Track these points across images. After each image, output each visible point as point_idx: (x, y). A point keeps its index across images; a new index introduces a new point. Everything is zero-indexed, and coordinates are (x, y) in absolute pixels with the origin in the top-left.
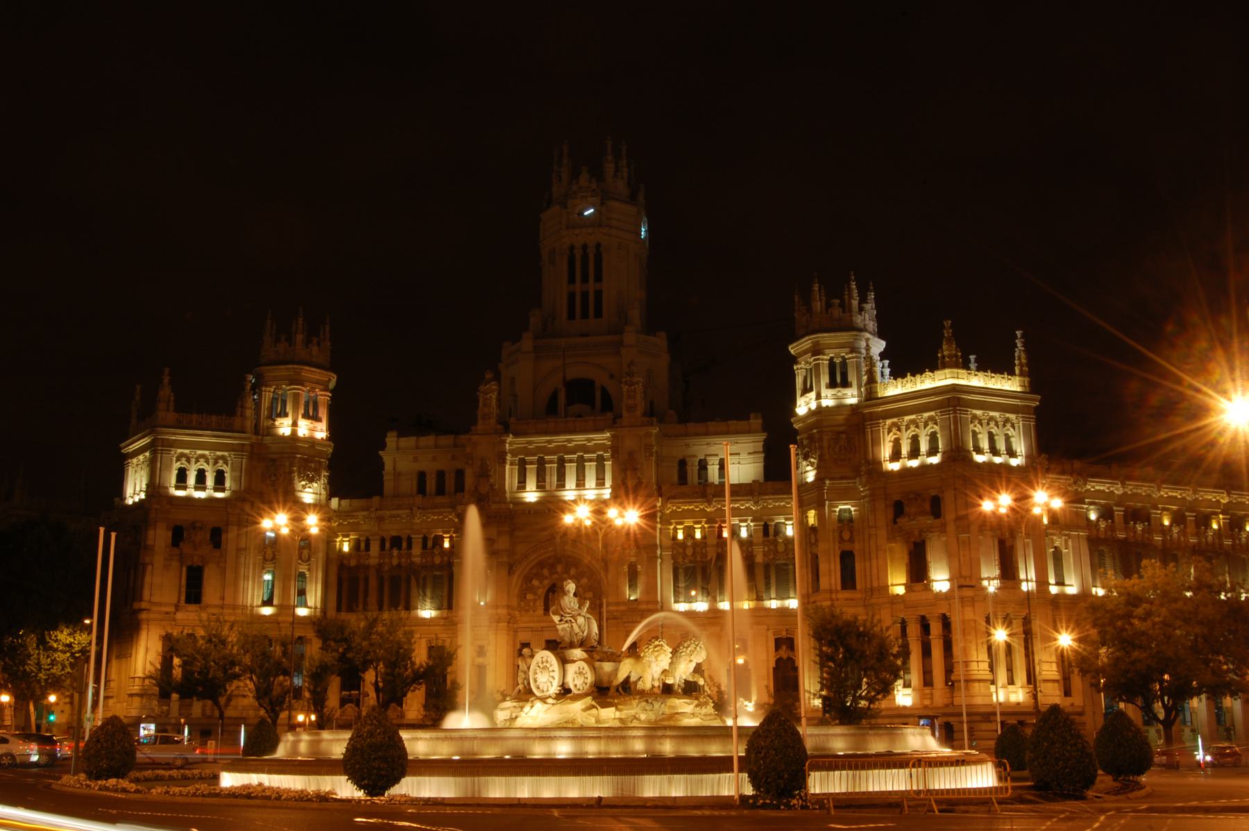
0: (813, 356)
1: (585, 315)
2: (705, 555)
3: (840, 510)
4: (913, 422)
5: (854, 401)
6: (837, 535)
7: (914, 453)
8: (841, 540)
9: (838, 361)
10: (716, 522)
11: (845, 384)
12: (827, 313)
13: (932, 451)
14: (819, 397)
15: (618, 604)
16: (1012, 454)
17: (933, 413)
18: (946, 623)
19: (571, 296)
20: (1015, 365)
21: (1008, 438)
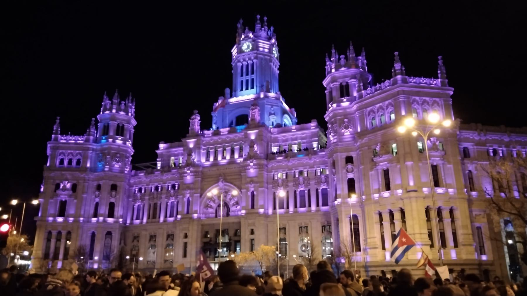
0: (332, 83)
4: (381, 107)
9: (344, 84)
10: (292, 170)
12: (339, 62)
17: (390, 101)
18: (402, 212)
19: (242, 82)
20: (438, 74)
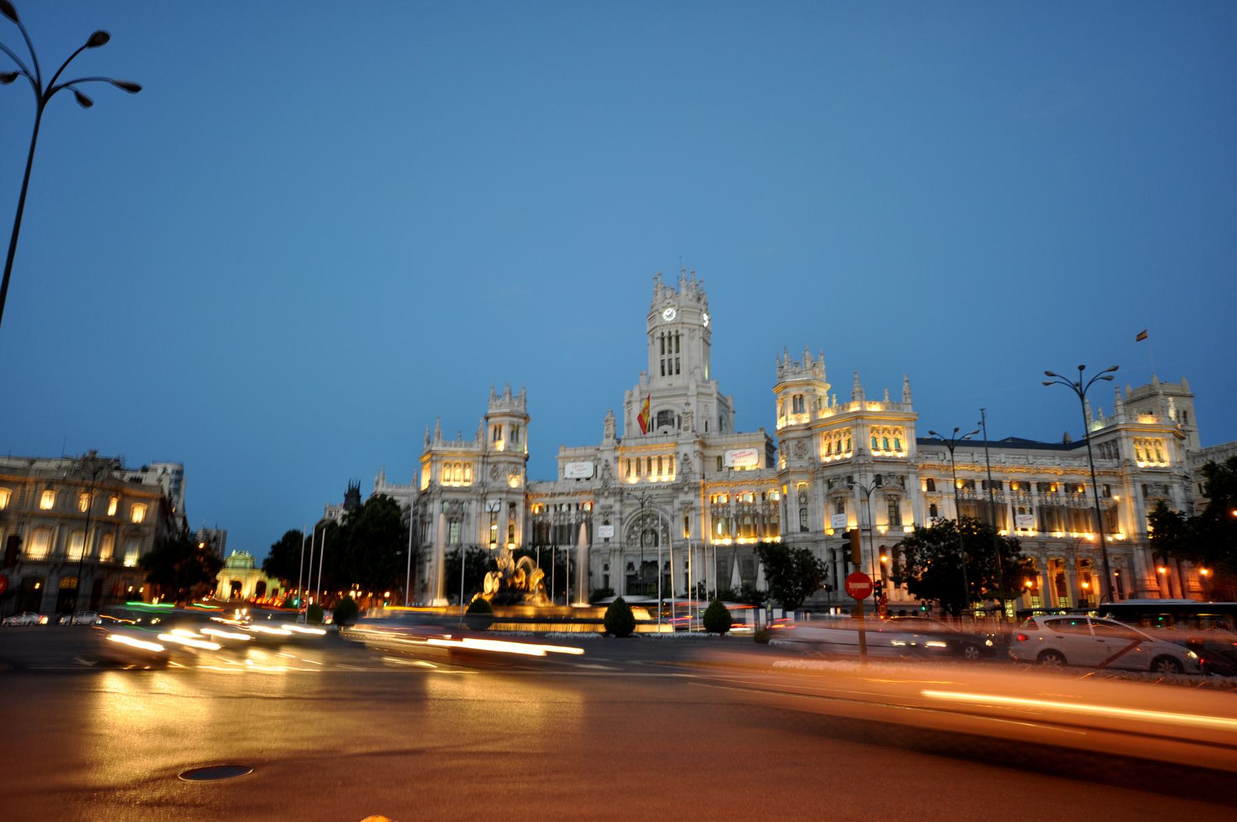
1: (670, 373)
2: (729, 512)
3: (800, 485)
4: (838, 432)
5: (807, 421)
6: (797, 499)
7: (839, 451)
8: (800, 503)
11: (802, 411)
13: (848, 451)
14: (787, 420)
15: (679, 541)
16: (899, 449)
21: (897, 440)
